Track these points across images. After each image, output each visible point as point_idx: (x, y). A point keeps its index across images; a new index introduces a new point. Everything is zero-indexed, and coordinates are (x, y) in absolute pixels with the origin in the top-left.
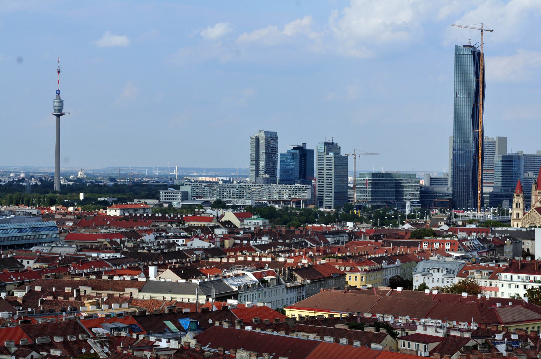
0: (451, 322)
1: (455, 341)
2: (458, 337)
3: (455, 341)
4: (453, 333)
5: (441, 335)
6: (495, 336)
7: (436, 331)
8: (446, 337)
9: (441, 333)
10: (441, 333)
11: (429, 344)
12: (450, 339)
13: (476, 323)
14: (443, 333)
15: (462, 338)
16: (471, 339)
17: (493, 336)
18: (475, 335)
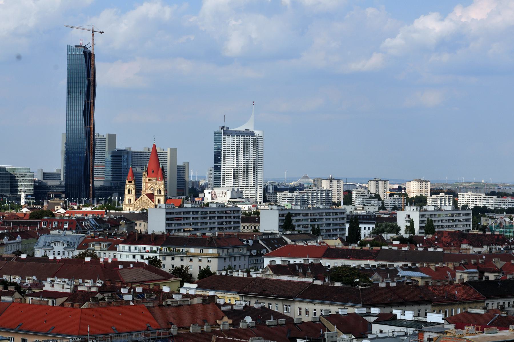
0: (77, 281)
1: (82, 295)
2: (85, 291)
3: (82, 295)
4: (80, 288)
5: (68, 291)
6: (121, 291)
7: (63, 287)
8: (74, 292)
9: (68, 289)
10: (68, 289)
11: (57, 299)
12: (77, 294)
13: (101, 280)
14: (71, 288)
15: (90, 292)
16: (97, 293)
17: (118, 291)
18: (101, 290)
